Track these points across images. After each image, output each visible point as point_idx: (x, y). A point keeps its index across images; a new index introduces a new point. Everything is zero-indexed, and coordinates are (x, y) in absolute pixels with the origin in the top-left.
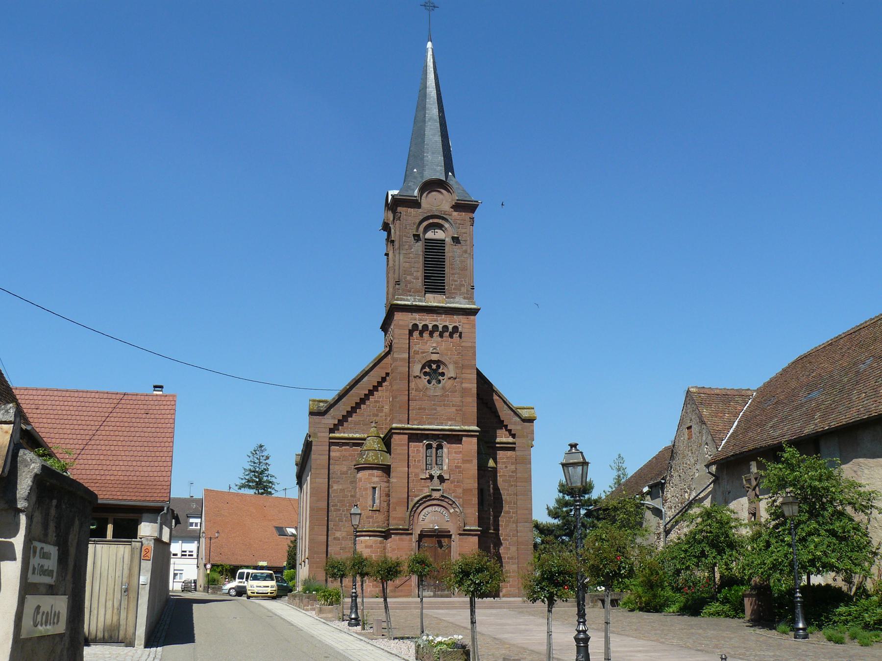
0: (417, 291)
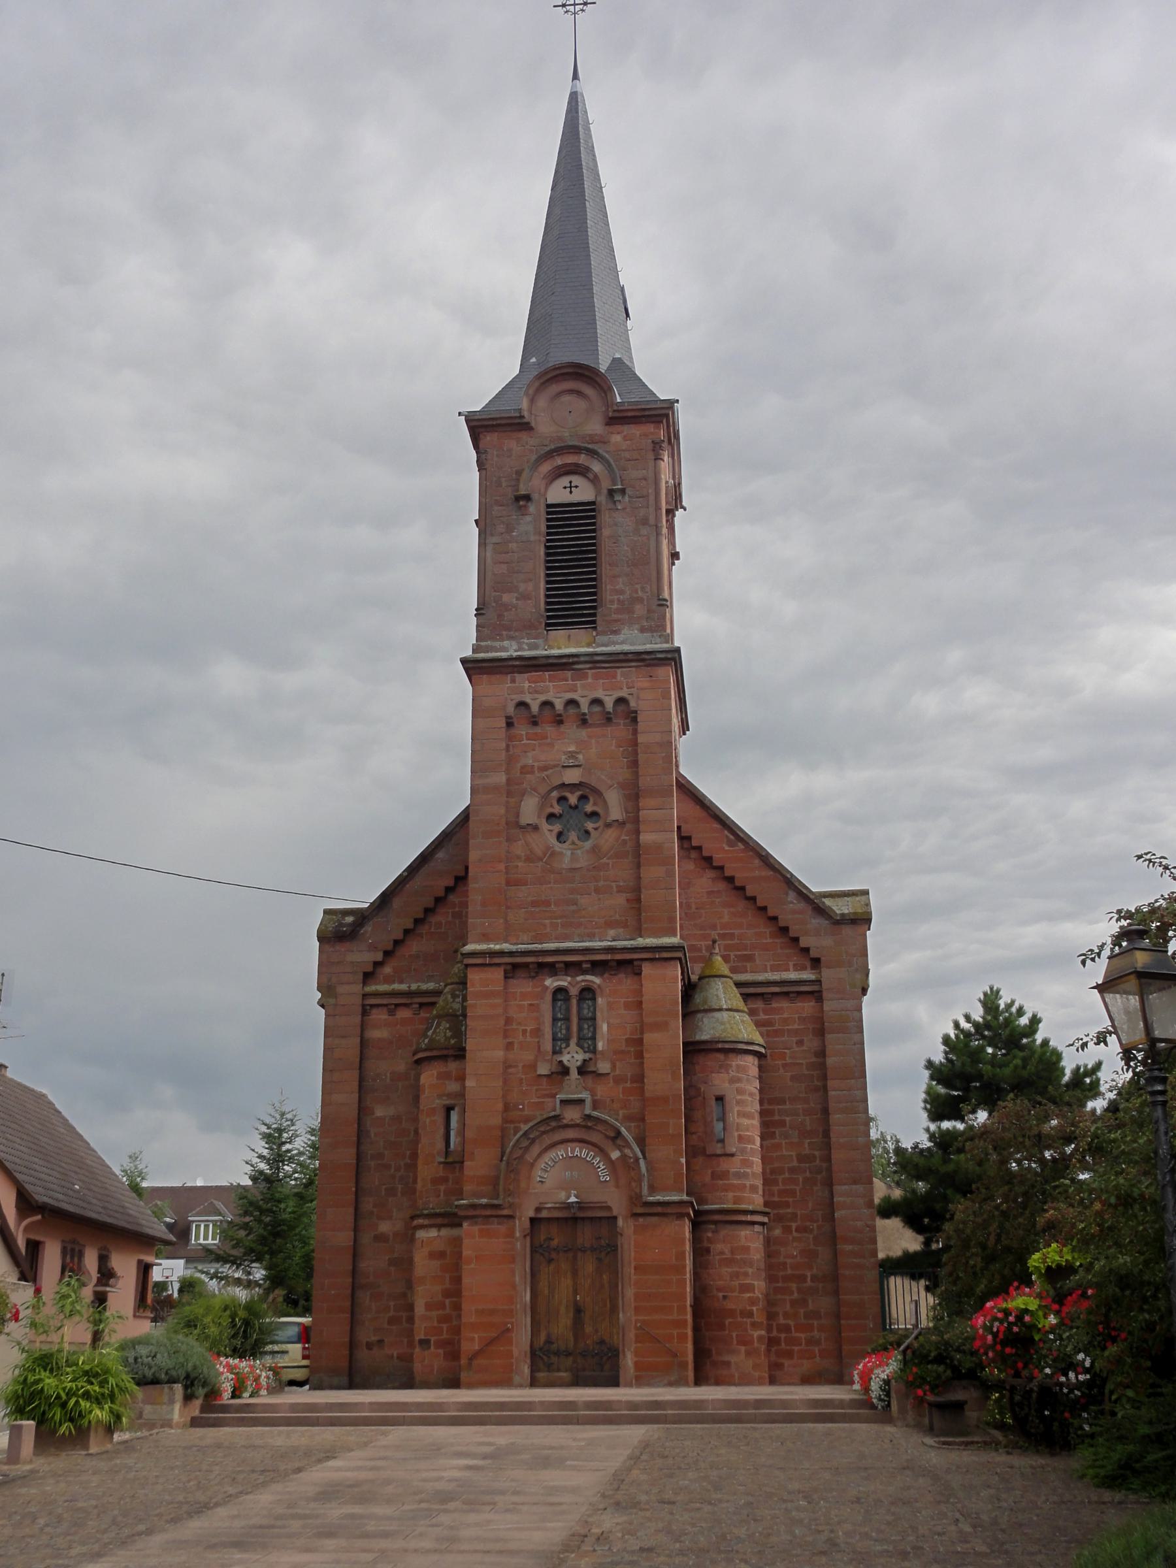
0: (528, 627)
